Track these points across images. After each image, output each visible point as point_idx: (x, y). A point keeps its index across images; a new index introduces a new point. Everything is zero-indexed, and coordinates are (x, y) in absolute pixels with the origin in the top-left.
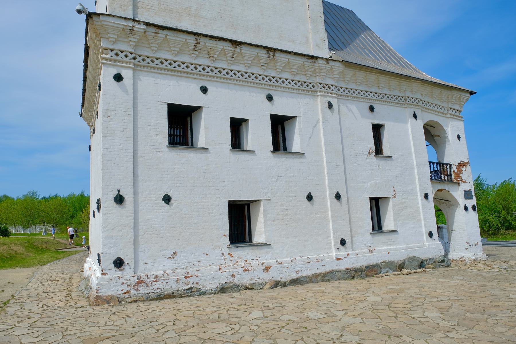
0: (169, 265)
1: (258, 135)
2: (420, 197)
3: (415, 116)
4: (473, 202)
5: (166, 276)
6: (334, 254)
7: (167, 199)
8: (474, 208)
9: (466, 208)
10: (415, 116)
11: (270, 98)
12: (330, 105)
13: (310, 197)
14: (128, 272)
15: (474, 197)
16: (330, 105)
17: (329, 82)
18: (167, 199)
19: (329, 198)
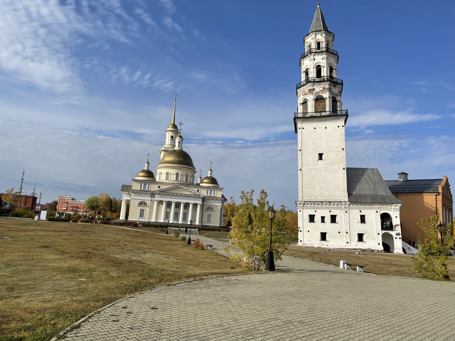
0: (309, 242)
1: (328, 219)
2: (376, 235)
3: (377, 212)
4: (400, 236)
5: (308, 244)
6: (345, 245)
7: (309, 231)
8: (400, 238)
9: (396, 238)
10: (377, 212)
11: (330, 211)
12: (346, 212)
13: (339, 232)
14: (302, 242)
15: (401, 235)
16: (346, 212)
17: (346, 206)
18: (309, 231)
19: (345, 233)
